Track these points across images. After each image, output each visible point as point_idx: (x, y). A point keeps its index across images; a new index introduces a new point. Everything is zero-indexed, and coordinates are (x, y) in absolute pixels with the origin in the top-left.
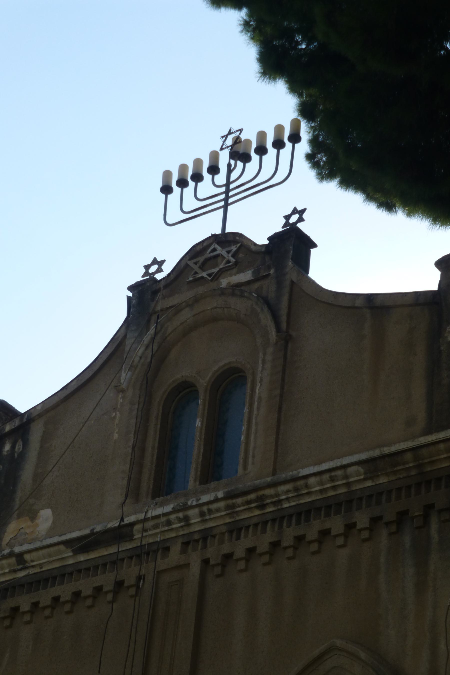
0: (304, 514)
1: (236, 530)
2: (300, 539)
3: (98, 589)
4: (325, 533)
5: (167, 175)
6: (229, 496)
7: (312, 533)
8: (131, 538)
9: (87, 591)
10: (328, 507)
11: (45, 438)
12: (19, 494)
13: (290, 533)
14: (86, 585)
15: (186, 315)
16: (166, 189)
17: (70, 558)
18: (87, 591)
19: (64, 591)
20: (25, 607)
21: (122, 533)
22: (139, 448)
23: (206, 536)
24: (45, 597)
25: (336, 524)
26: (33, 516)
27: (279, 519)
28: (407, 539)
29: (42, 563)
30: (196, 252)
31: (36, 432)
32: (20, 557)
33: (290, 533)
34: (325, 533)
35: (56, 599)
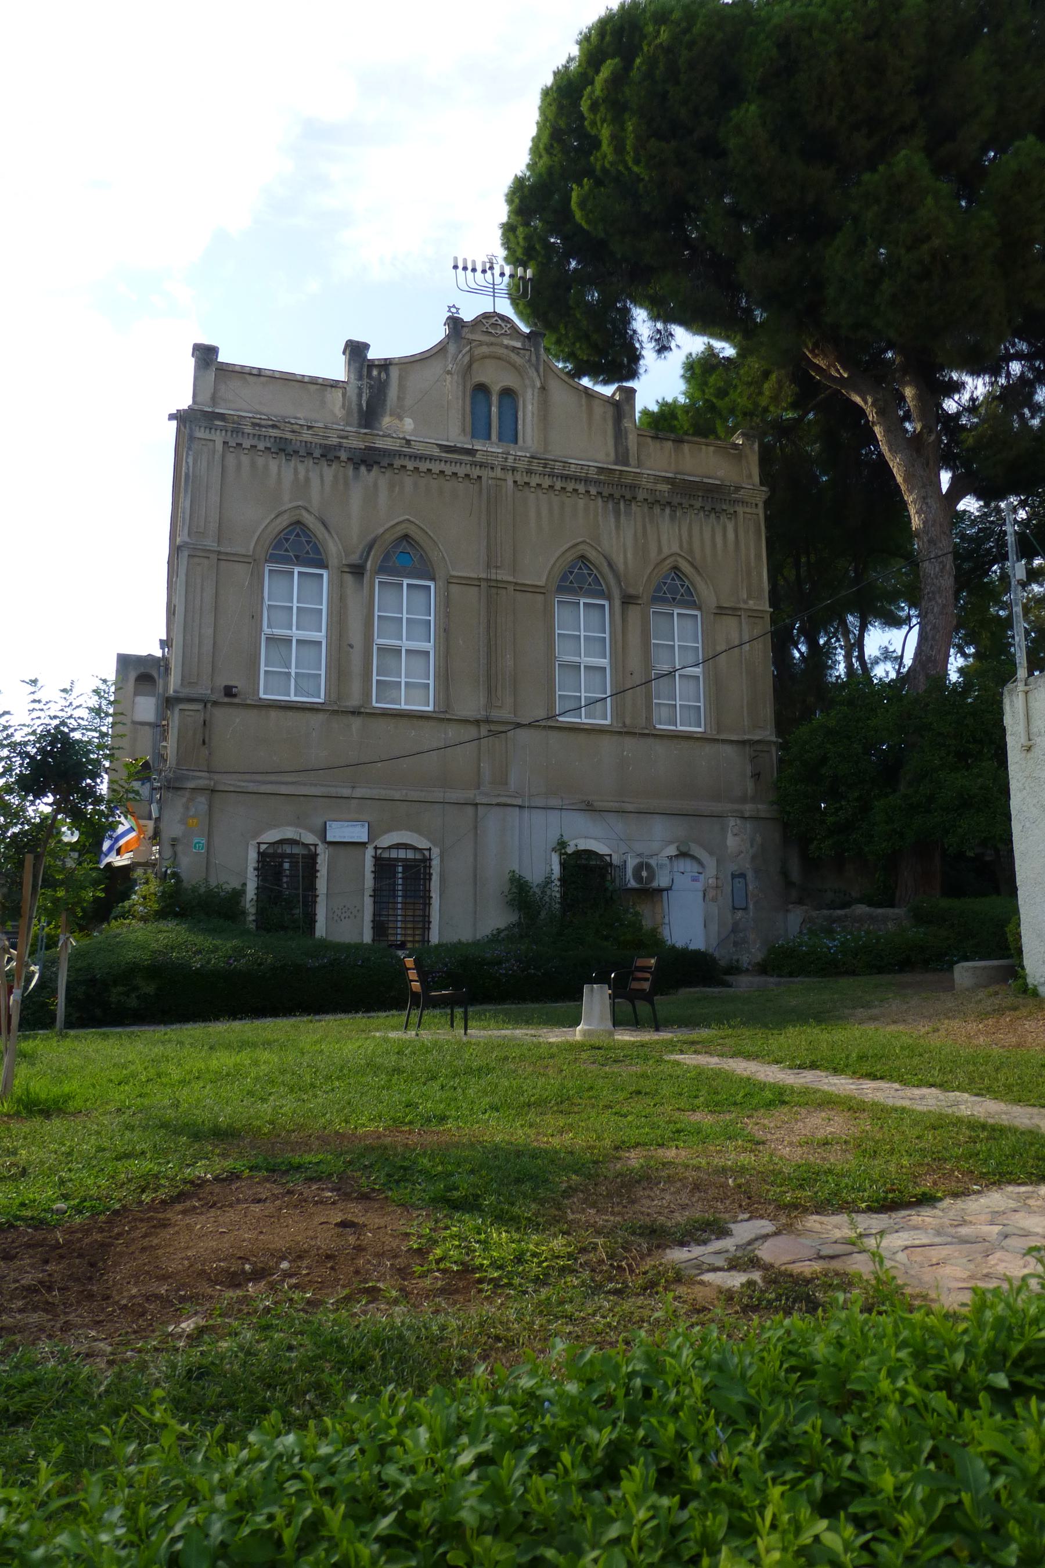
0: (566, 478)
1: (529, 472)
2: (563, 489)
3: (455, 474)
4: (575, 490)
5: (456, 259)
6: (532, 457)
7: (570, 488)
8: (474, 456)
9: (448, 472)
10: (577, 479)
11: (401, 378)
12: (389, 403)
13: (558, 485)
14: (449, 469)
15: (485, 350)
16: (456, 267)
17: (436, 452)
18: (448, 472)
19: (436, 467)
20: (410, 467)
21: (471, 452)
22: (464, 409)
23: (514, 469)
24: (424, 466)
25: (582, 489)
26: (401, 418)
27: (552, 475)
28: (610, 505)
29: (418, 449)
30: (486, 316)
31: (394, 373)
32: (408, 442)
33: (558, 485)
34: (575, 490)
35: (429, 470)
